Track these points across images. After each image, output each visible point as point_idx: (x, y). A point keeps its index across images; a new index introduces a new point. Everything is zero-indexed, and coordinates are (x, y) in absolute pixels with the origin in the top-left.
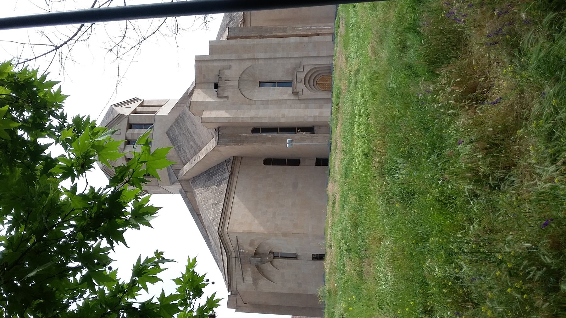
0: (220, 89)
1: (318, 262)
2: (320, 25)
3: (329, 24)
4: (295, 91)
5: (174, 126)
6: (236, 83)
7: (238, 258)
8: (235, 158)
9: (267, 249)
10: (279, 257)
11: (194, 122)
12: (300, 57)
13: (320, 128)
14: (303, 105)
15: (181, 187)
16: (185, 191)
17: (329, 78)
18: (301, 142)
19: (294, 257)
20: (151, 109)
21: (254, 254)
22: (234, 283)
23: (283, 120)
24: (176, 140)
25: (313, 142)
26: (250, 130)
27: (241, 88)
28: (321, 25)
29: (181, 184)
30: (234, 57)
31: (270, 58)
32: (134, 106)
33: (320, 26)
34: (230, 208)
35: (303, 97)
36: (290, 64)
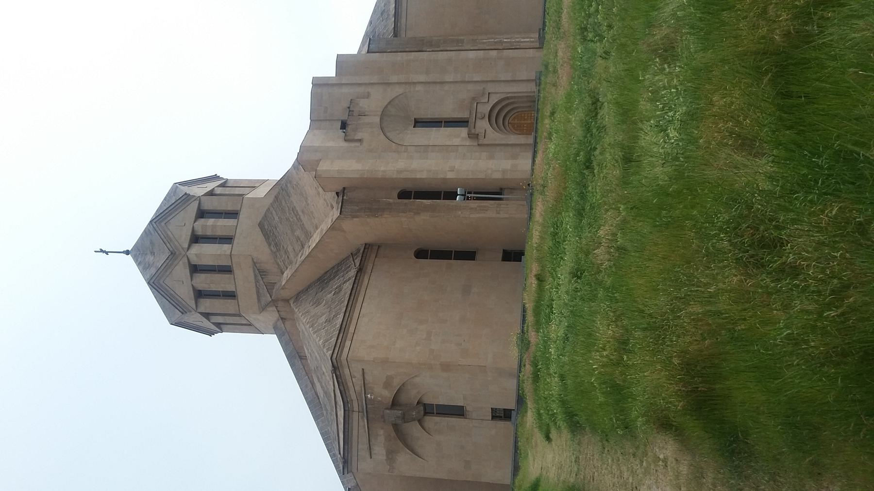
0: (349, 128)
1: (501, 424)
3: (532, 36)
4: (473, 131)
5: (271, 209)
6: (377, 119)
7: (363, 412)
8: (368, 247)
9: (411, 396)
10: (434, 413)
11: (304, 193)
12: (483, 82)
14: (485, 153)
15: (276, 315)
16: (282, 319)
17: (529, 115)
19: (458, 412)
20: (237, 191)
21: (391, 403)
22: (354, 458)
23: (450, 175)
24: (273, 233)
25: (499, 213)
26: (396, 195)
28: (518, 36)
29: (276, 307)
30: (375, 79)
31: (435, 83)
32: (210, 186)
33: (518, 38)
34: (354, 322)
35: (485, 142)
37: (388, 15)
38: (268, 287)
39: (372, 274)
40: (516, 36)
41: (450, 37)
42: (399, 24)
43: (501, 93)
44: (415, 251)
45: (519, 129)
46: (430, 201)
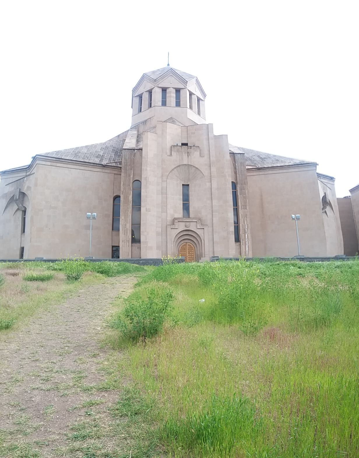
2: (250, 242)
3: (251, 252)
6: (185, 162)
13: (138, 248)
14: (161, 230)
17: (193, 255)
18: (122, 230)
25: (123, 242)
27: (180, 167)
28: (250, 244)
33: (248, 243)
36: (205, 214)
37: (274, 164)
38: (137, 126)
39: (102, 173)
40: (250, 242)
41: (248, 200)
42: (268, 170)
43: (204, 235)
44: (117, 195)
45: (182, 250)
46: (131, 199)
